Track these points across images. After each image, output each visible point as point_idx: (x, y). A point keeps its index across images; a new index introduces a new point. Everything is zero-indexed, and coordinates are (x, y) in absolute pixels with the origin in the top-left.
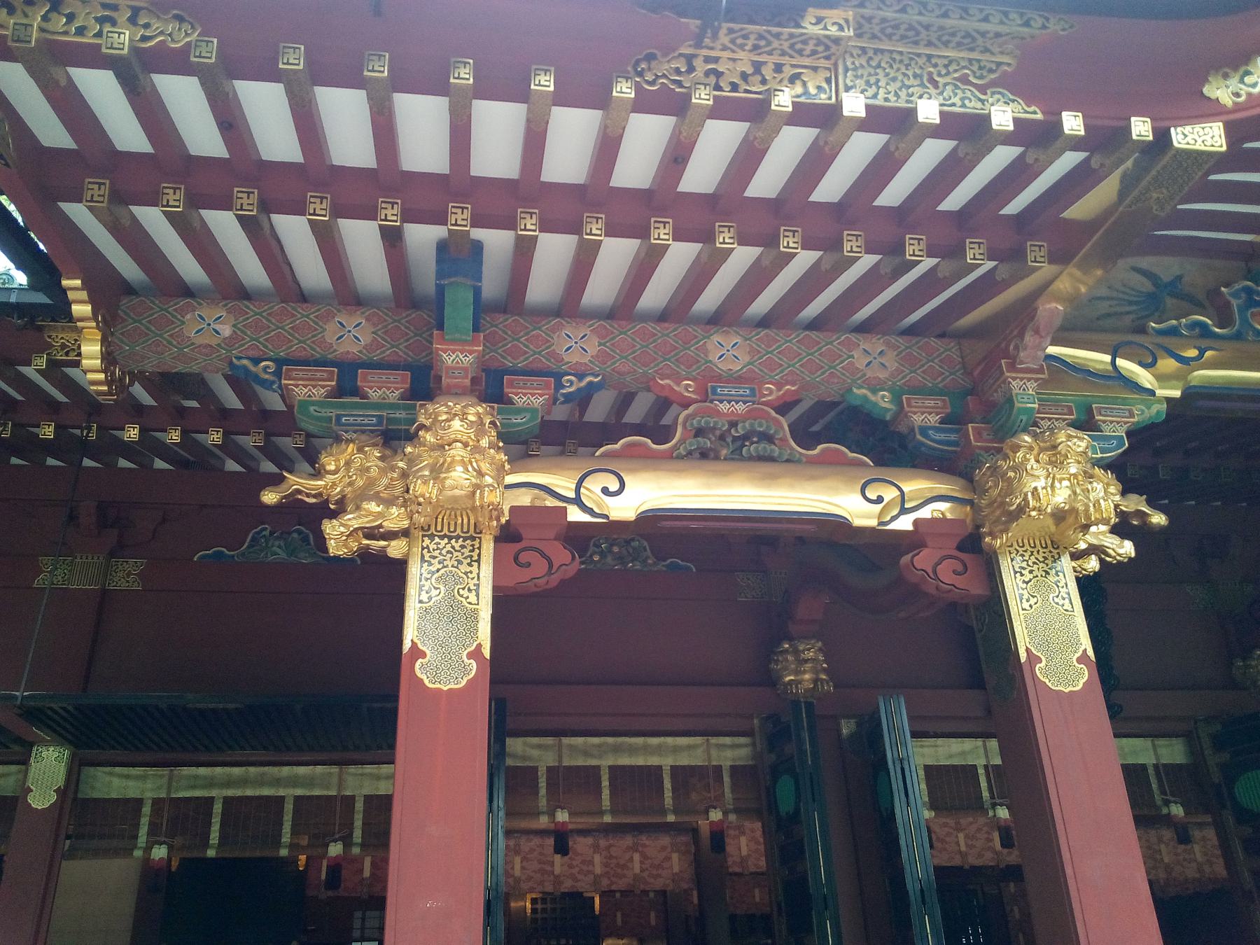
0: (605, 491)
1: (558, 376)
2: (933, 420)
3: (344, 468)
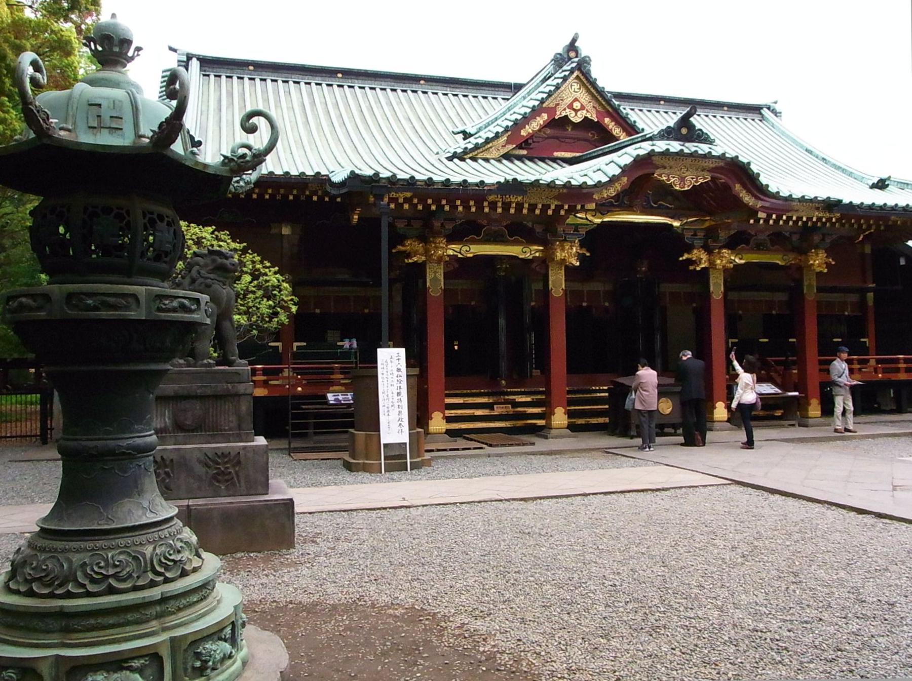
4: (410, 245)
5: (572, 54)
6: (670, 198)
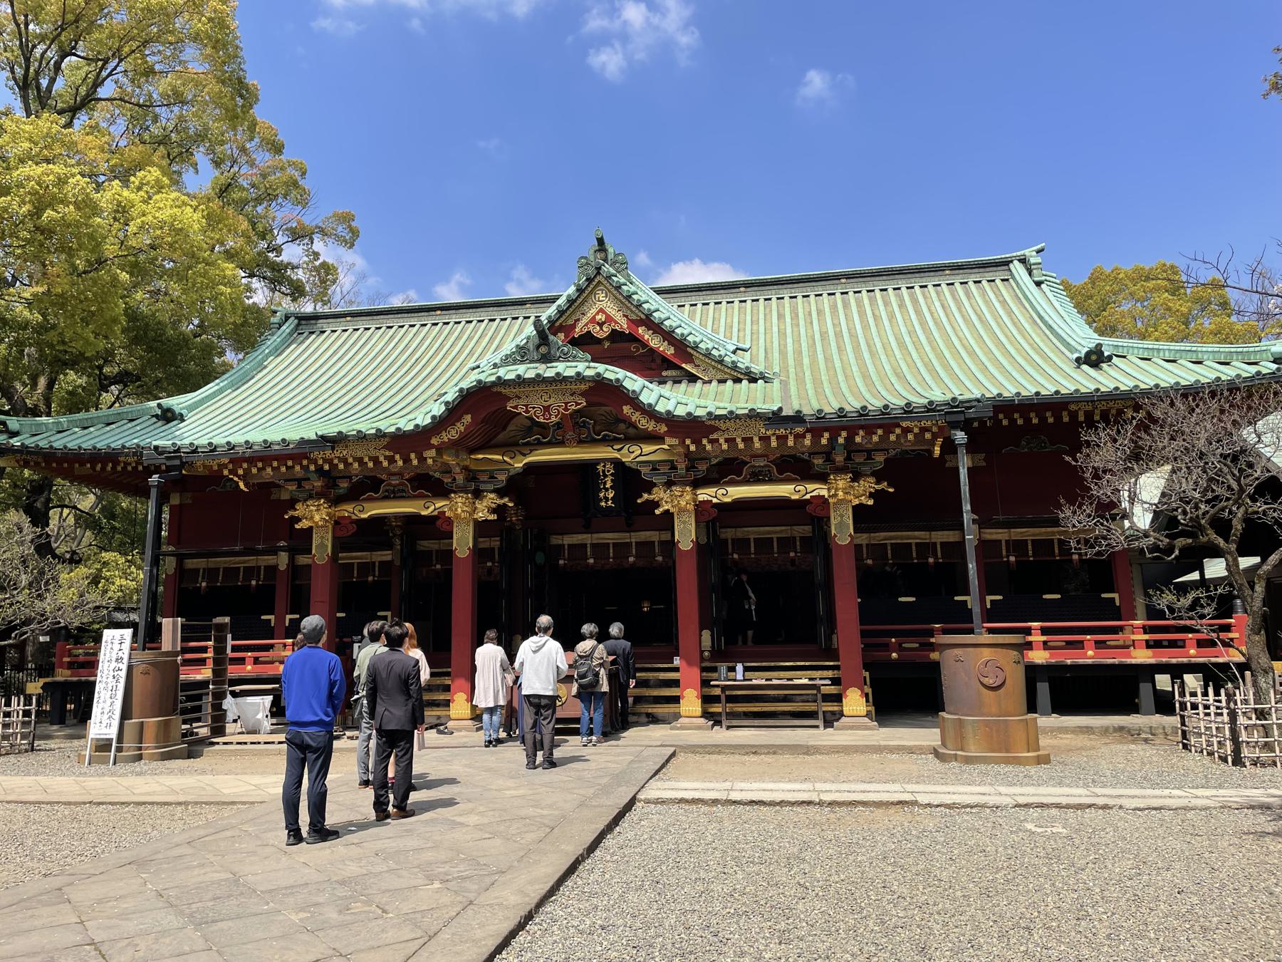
1: (350, 478)
6: (622, 426)
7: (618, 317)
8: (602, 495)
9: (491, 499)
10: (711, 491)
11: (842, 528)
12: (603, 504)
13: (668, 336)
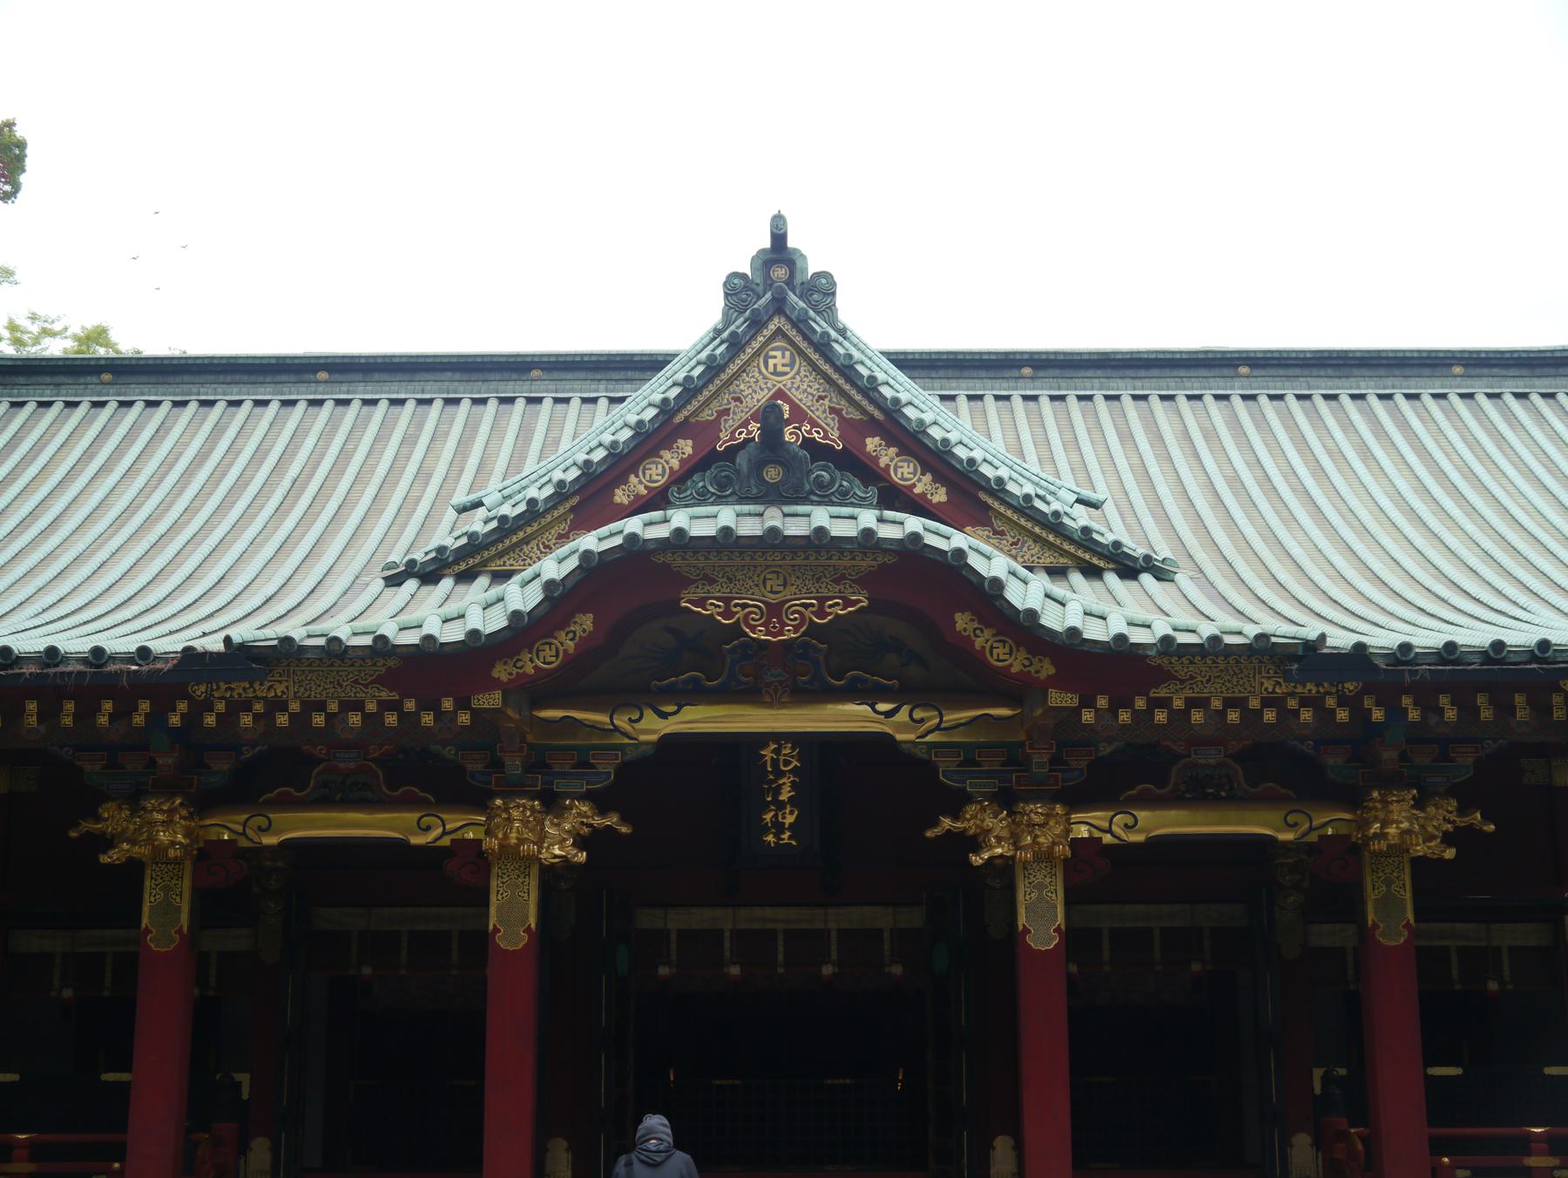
0: (260, 828)
2: (480, 767)
3: (113, 818)
4: (113, 818)
5: (780, 273)
7: (819, 412)
8: (768, 817)
9: (581, 815)
10: (1099, 817)
11: (1391, 910)
12: (770, 838)
13: (937, 460)
